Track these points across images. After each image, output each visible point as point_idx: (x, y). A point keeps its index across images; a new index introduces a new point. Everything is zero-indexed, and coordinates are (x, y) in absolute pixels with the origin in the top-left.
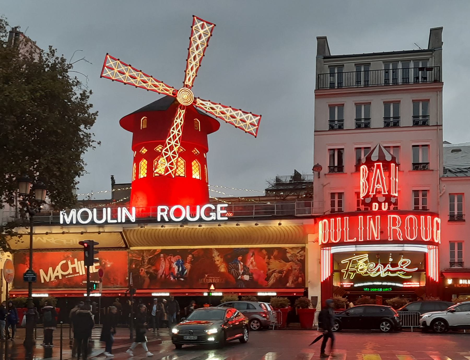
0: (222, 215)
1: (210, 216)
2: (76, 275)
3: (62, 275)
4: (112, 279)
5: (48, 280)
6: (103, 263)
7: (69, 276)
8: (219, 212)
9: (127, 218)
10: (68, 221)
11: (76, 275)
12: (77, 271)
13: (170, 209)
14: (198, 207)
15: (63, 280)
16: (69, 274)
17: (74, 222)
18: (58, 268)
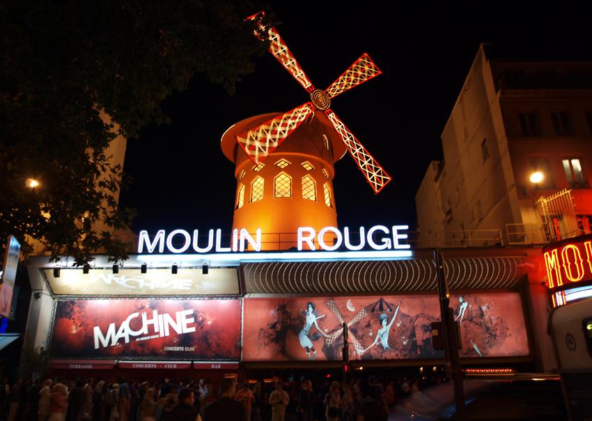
0: (401, 242)
1: (384, 243)
2: (153, 337)
3: (130, 336)
4: (214, 344)
5: (105, 344)
6: (201, 319)
7: (142, 339)
8: (396, 237)
9: (246, 242)
10: (151, 248)
11: (153, 337)
12: (156, 330)
13: (317, 233)
14: (362, 229)
15: (132, 344)
16: (142, 335)
17: (161, 249)
18: (125, 325)
